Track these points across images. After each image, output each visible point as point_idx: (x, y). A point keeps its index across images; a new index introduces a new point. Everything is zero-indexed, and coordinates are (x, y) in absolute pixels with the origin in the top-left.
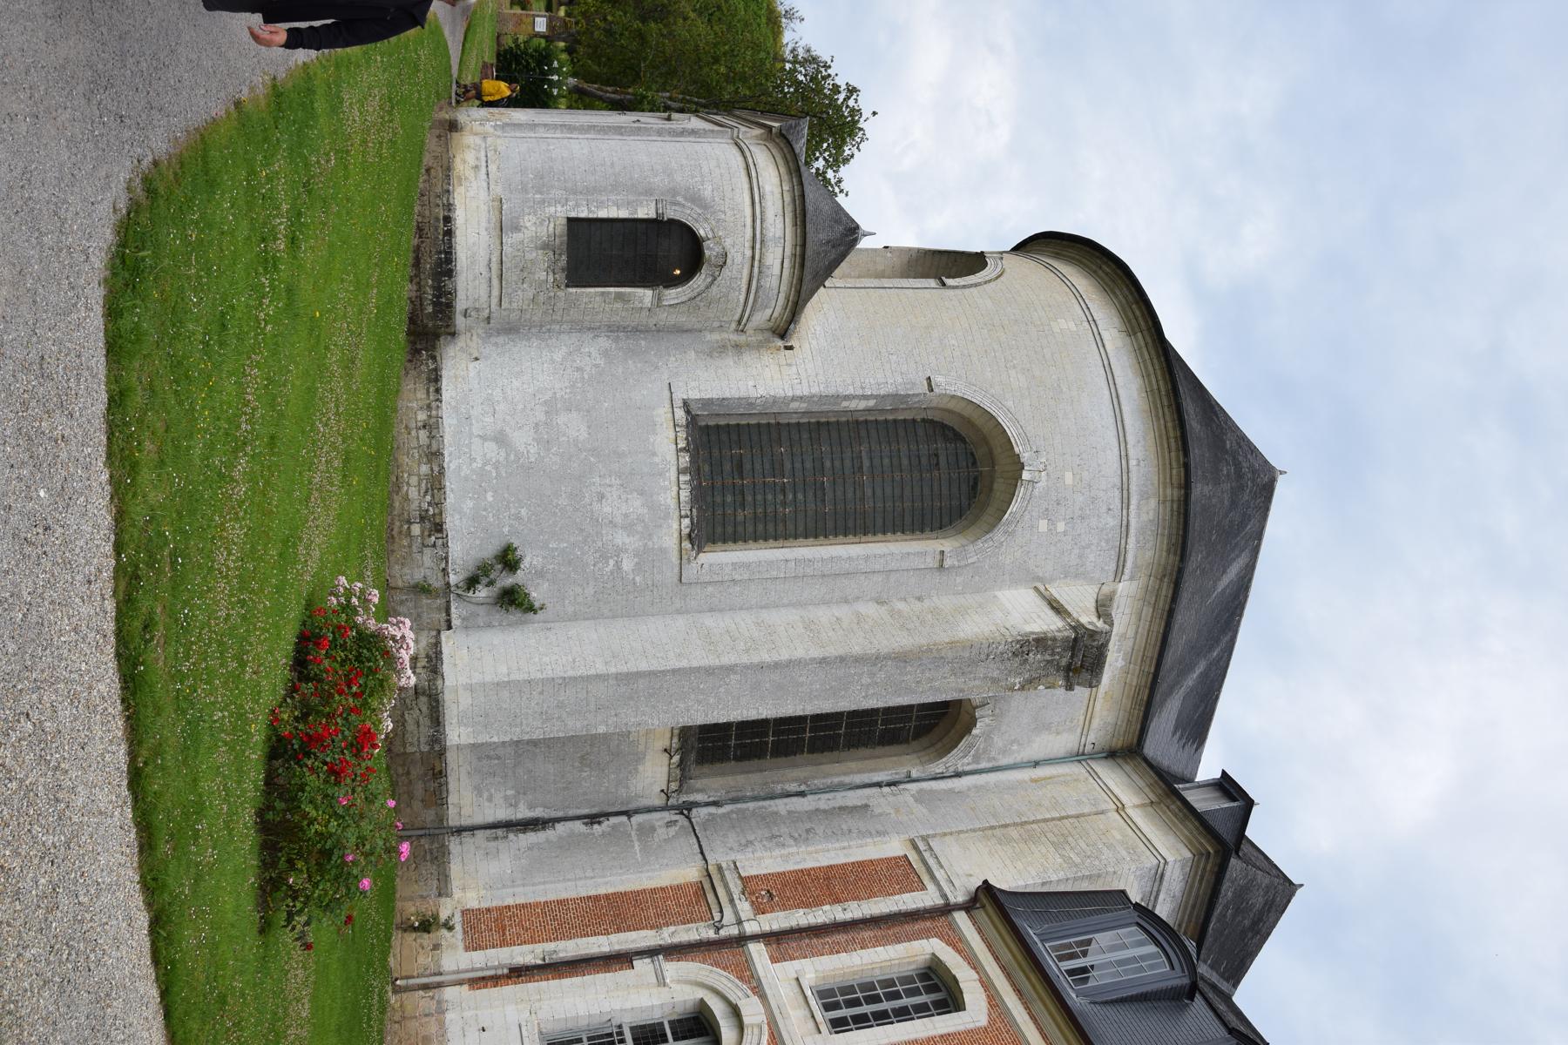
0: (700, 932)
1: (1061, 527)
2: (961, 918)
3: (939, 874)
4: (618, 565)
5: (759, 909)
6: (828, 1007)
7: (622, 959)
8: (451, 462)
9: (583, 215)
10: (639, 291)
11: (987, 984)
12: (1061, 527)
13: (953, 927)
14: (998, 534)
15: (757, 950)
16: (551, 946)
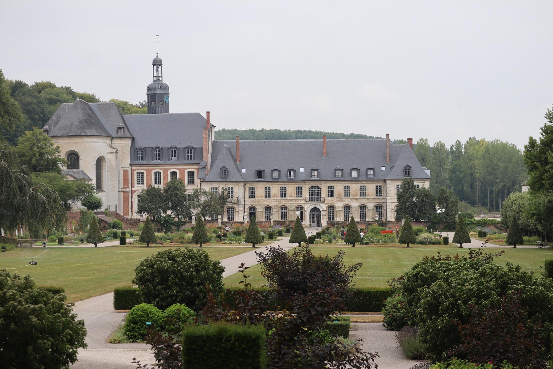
0: (130, 194)
2: (132, 168)
3: (127, 168)
5: (128, 187)
6: (139, 184)
7: (132, 202)
11: (141, 169)
13: (133, 169)
15: (133, 189)
16: (129, 208)
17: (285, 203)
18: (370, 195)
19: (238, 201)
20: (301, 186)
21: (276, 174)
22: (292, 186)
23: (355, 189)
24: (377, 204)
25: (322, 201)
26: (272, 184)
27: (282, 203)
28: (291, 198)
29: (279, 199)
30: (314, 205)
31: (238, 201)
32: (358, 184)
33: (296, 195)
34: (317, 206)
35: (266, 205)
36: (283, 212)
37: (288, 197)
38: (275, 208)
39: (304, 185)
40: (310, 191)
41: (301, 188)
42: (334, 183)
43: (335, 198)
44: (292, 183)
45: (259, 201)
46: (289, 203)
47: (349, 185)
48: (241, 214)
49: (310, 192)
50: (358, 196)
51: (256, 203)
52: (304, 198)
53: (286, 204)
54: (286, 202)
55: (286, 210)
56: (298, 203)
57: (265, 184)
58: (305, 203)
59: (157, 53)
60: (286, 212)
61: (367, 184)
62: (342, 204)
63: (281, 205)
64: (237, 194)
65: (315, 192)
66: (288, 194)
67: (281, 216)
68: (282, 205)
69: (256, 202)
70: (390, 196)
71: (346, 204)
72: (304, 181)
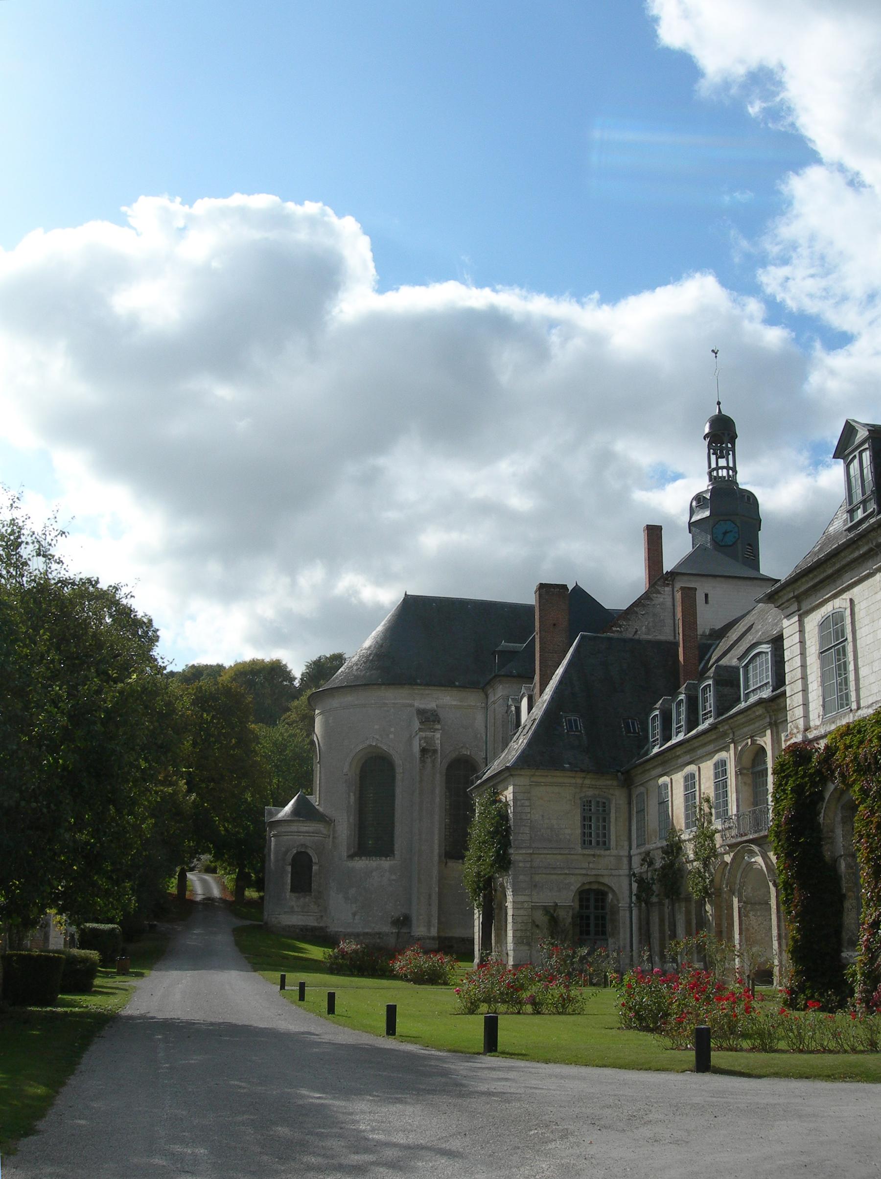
1: (392, 729)
4: (393, 880)
8: (360, 930)
9: (289, 887)
10: (313, 870)
12: (392, 729)
14: (392, 752)
59: (719, 403)
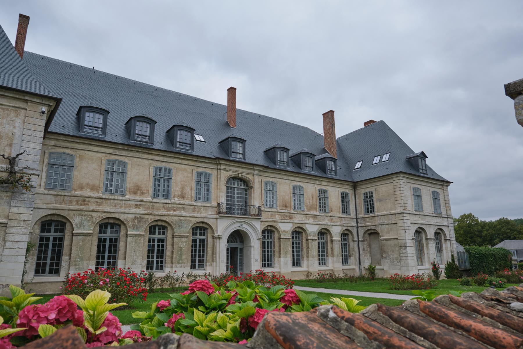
17: (166, 213)
18: (333, 209)
19: (12, 173)
20: (209, 171)
21: (142, 129)
22: (185, 170)
23: (310, 196)
24: (344, 228)
25: (255, 215)
26: (132, 154)
27: (157, 213)
28: (182, 201)
29: (150, 199)
30: (238, 225)
31: (12, 173)
32: (316, 186)
33: (194, 194)
34: (246, 228)
35: (105, 216)
36: (154, 240)
37: (174, 197)
38: (134, 226)
39: (215, 172)
40: (227, 188)
41: (208, 176)
42: (277, 176)
43: (279, 210)
44: (187, 162)
45: (84, 200)
46: (177, 213)
47: (301, 184)
48: (17, 238)
49: (227, 192)
50: (316, 209)
51: (71, 207)
52: (216, 204)
53: (169, 215)
54: (169, 209)
55: (163, 233)
56: (199, 215)
57: (111, 151)
58: (217, 216)
60: (163, 240)
61: (328, 188)
62: (291, 225)
63: (153, 218)
64: (11, 145)
65: (236, 191)
66: (175, 189)
67: (149, 251)
68: (157, 218)
69: (71, 202)
70: (408, 208)
71: (298, 225)
72: (216, 161)
